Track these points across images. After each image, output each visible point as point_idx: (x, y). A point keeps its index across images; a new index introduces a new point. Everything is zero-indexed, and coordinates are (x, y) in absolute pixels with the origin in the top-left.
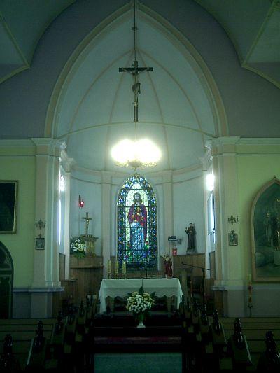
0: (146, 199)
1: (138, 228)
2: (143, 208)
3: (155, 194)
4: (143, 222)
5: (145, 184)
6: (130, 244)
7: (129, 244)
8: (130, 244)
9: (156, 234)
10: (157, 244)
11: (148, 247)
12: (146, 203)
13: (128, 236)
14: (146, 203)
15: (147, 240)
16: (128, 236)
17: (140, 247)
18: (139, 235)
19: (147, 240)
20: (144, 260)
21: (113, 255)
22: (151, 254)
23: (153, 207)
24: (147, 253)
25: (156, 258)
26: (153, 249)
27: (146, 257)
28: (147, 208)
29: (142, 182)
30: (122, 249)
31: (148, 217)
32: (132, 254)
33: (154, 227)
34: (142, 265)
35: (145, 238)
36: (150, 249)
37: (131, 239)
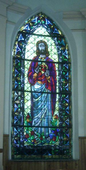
0: (55, 51)
1: (42, 93)
2: (50, 63)
3: (69, 44)
4: (51, 85)
5: (53, 30)
6: (31, 116)
7: (28, 117)
8: (31, 116)
9: (70, 103)
10: (71, 119)
11: (58, 123)
12: (54, 56)
13: (28, 104)
14: (54, 56)
15: (56, 113)
16: (28, 104)
17: (45, 123)
18: (45, 105)
19: (56, 113)
20: (52, 143)
21: (7, 132)
22: (62, 133)
23: (65, 63)
24: (56, 132)
25: (70, 139)
26: (64, 129)
27: (54, 138)
28: (57, 65)
29: (49, 26)
30: (17, 125)
31: (58, 78)
32: (33, 133)
33: (66, 93)
34: (49, 150)
35: (53, 109)
36: (61, 126)
37: (32, 109)
